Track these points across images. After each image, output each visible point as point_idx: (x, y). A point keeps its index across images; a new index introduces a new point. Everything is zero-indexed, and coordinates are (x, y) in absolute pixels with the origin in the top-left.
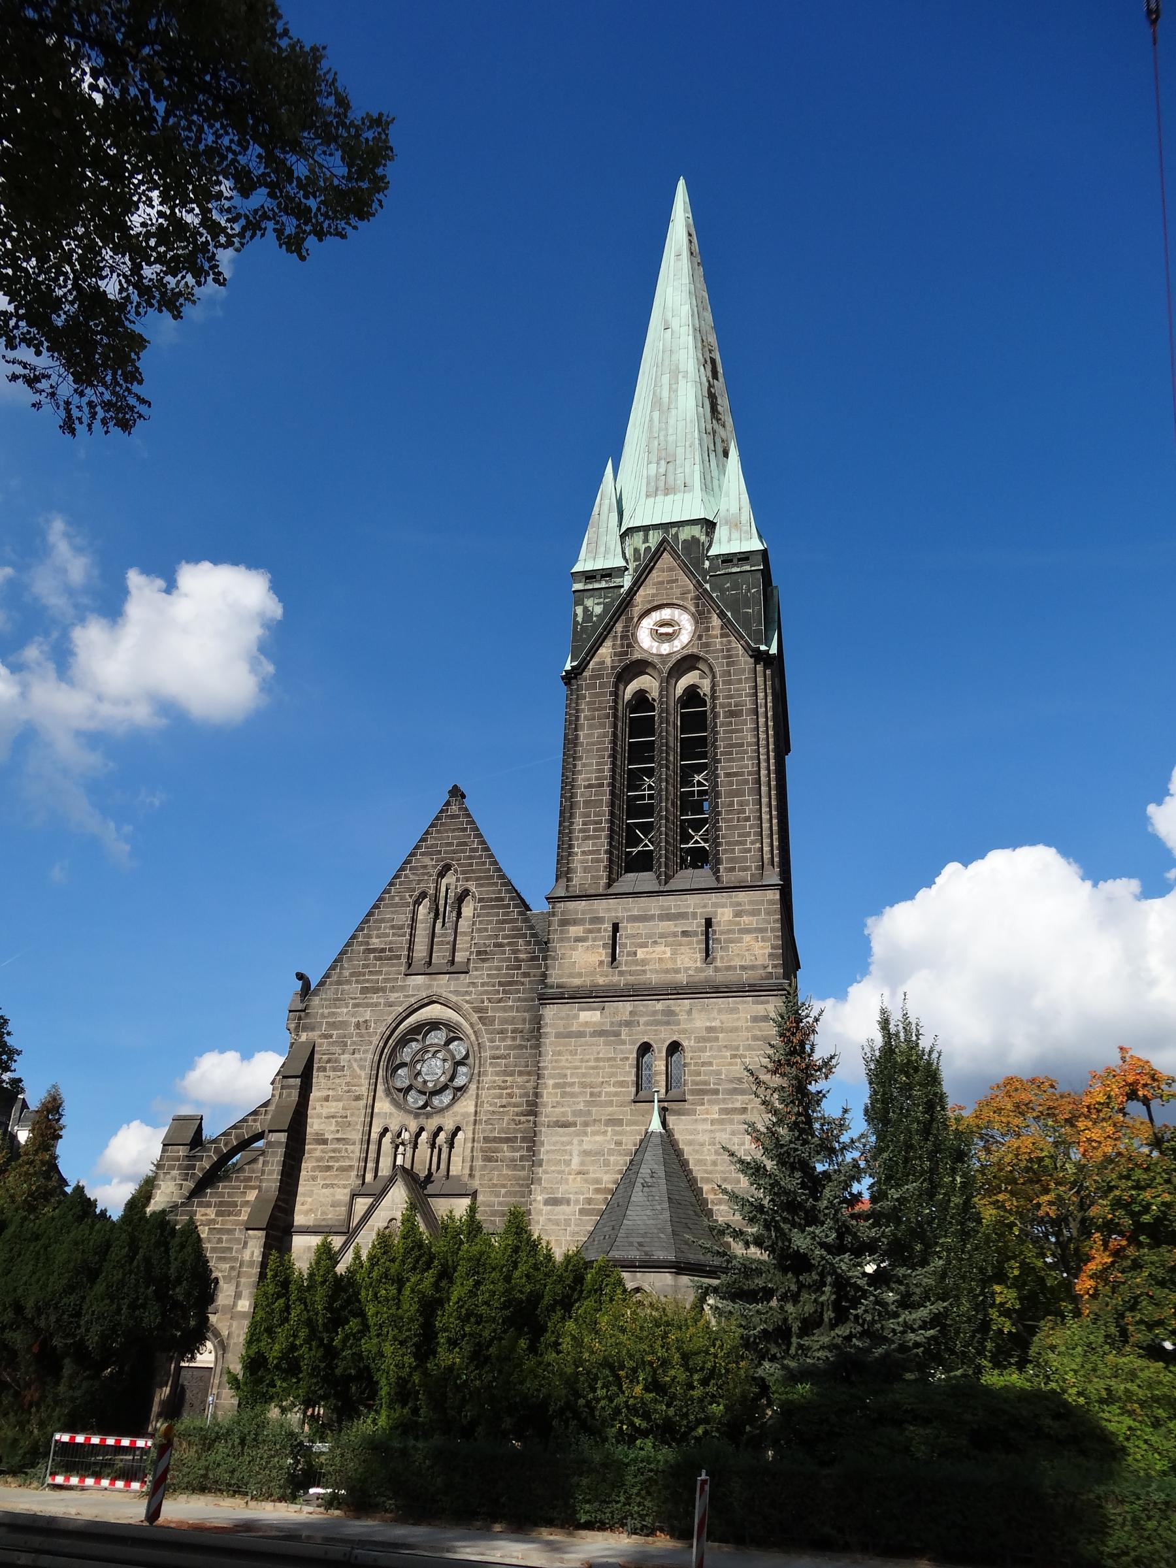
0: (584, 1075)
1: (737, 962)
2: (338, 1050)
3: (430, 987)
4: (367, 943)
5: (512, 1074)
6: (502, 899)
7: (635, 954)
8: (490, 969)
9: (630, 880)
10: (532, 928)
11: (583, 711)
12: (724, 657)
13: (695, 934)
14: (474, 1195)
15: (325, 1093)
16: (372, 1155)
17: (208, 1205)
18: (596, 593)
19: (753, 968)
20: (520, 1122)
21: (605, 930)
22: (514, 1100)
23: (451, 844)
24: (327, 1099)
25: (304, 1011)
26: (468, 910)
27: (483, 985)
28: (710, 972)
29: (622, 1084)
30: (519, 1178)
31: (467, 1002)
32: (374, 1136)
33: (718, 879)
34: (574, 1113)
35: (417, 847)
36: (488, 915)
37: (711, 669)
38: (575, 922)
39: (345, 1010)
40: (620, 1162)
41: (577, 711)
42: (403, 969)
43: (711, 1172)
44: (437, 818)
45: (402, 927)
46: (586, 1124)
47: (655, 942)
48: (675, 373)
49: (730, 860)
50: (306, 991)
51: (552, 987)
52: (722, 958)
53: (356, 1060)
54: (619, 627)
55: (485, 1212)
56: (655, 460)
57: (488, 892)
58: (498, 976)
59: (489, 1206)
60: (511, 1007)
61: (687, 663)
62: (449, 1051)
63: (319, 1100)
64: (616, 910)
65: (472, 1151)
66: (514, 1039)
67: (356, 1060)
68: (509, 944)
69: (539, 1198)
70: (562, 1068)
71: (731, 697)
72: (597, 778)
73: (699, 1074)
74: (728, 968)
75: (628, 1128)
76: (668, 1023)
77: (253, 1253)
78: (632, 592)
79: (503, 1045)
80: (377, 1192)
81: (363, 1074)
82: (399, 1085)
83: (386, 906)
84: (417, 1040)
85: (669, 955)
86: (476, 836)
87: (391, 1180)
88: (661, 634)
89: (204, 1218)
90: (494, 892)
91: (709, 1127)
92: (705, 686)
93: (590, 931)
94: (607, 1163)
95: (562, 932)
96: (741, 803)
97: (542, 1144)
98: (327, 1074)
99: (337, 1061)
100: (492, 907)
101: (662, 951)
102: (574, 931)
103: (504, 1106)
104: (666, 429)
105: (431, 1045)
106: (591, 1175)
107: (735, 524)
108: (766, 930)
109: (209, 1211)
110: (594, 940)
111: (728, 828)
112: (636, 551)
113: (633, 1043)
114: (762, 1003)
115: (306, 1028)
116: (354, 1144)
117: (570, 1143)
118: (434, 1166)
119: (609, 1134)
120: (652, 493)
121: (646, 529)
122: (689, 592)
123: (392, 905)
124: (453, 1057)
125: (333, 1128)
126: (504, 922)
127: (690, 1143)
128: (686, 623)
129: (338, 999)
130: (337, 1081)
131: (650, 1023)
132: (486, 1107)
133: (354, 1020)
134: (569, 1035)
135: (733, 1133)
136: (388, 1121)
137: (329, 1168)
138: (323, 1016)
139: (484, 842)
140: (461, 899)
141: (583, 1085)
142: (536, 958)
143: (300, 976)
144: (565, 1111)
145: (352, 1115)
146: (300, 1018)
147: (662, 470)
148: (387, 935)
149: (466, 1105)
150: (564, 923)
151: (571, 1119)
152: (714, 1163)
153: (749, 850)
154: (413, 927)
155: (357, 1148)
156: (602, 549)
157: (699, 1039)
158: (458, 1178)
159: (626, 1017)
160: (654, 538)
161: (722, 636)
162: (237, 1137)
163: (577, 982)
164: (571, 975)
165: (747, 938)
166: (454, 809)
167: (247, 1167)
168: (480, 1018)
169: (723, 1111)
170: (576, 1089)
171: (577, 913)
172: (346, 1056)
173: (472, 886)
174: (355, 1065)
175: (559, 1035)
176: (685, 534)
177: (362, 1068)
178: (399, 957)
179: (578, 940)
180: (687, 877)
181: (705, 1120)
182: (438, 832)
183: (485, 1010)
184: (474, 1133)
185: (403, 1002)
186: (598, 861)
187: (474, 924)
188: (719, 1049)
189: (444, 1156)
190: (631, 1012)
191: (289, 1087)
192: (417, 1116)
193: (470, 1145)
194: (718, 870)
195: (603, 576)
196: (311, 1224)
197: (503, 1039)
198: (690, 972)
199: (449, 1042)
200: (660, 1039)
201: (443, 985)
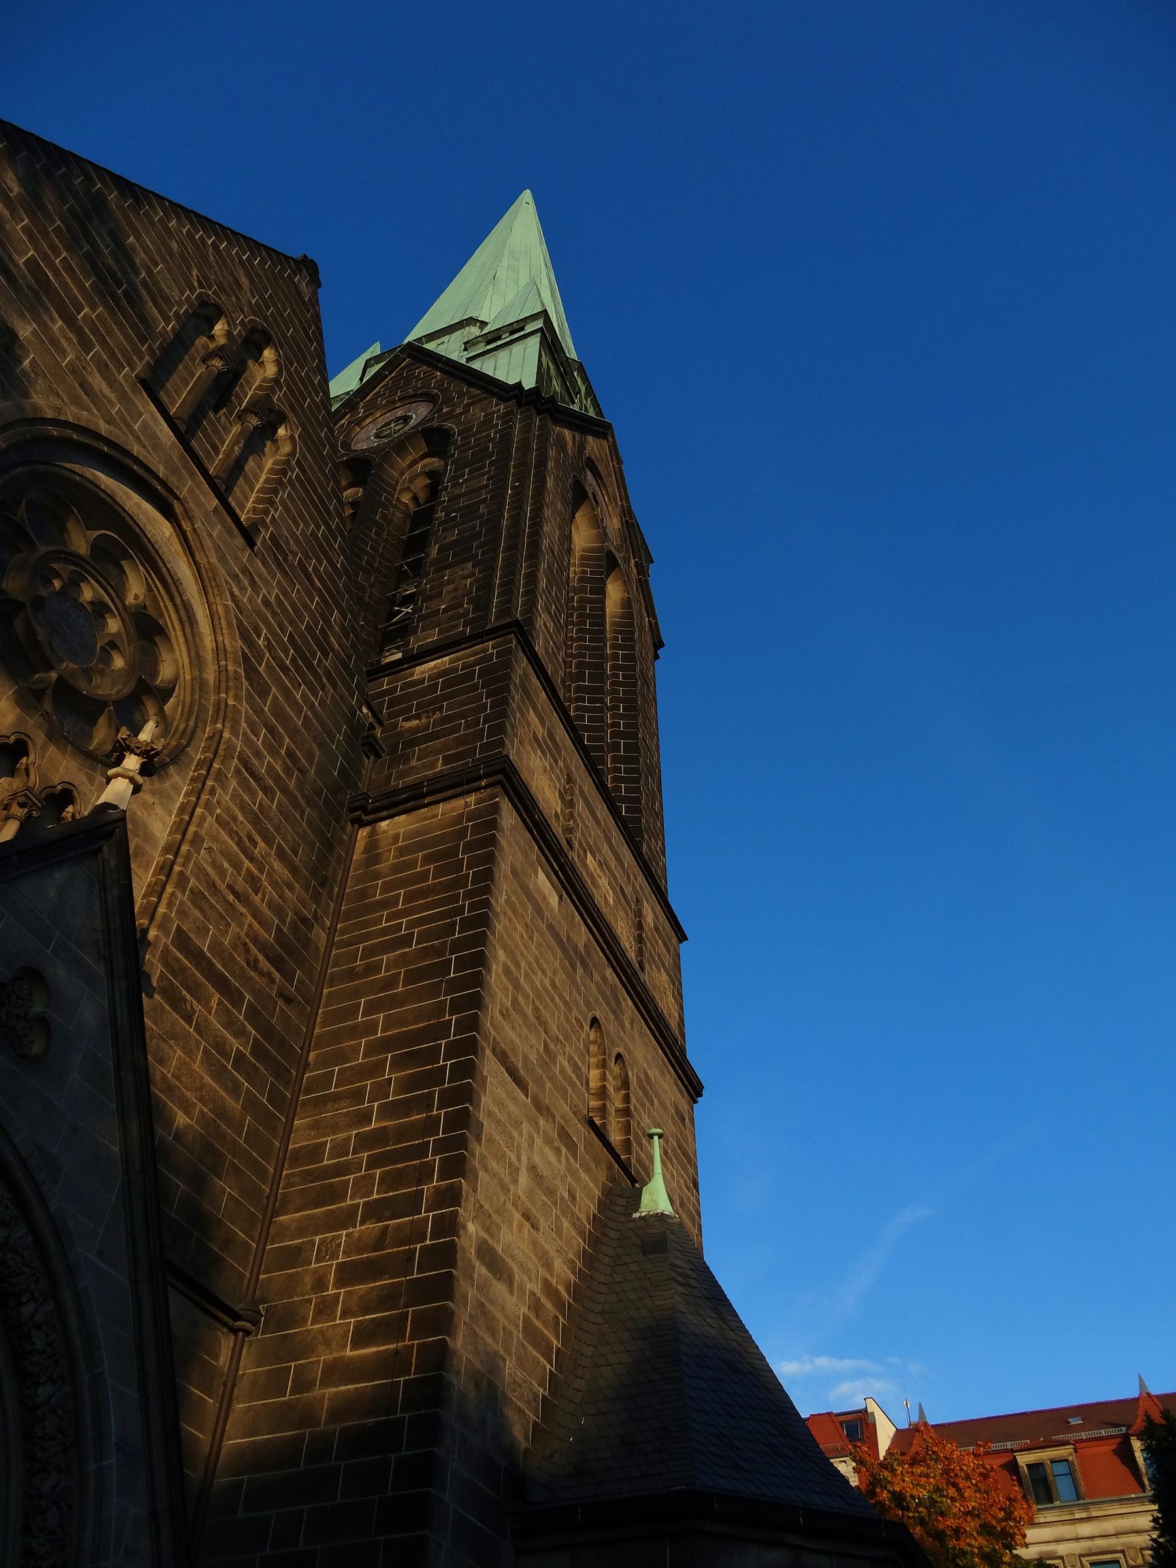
5: (269, 841)
20: (254, 965)
27: (266, 602)
45: (167, 300)
66: (287, 770)
69: (471, 1227)
197: (274, 752)
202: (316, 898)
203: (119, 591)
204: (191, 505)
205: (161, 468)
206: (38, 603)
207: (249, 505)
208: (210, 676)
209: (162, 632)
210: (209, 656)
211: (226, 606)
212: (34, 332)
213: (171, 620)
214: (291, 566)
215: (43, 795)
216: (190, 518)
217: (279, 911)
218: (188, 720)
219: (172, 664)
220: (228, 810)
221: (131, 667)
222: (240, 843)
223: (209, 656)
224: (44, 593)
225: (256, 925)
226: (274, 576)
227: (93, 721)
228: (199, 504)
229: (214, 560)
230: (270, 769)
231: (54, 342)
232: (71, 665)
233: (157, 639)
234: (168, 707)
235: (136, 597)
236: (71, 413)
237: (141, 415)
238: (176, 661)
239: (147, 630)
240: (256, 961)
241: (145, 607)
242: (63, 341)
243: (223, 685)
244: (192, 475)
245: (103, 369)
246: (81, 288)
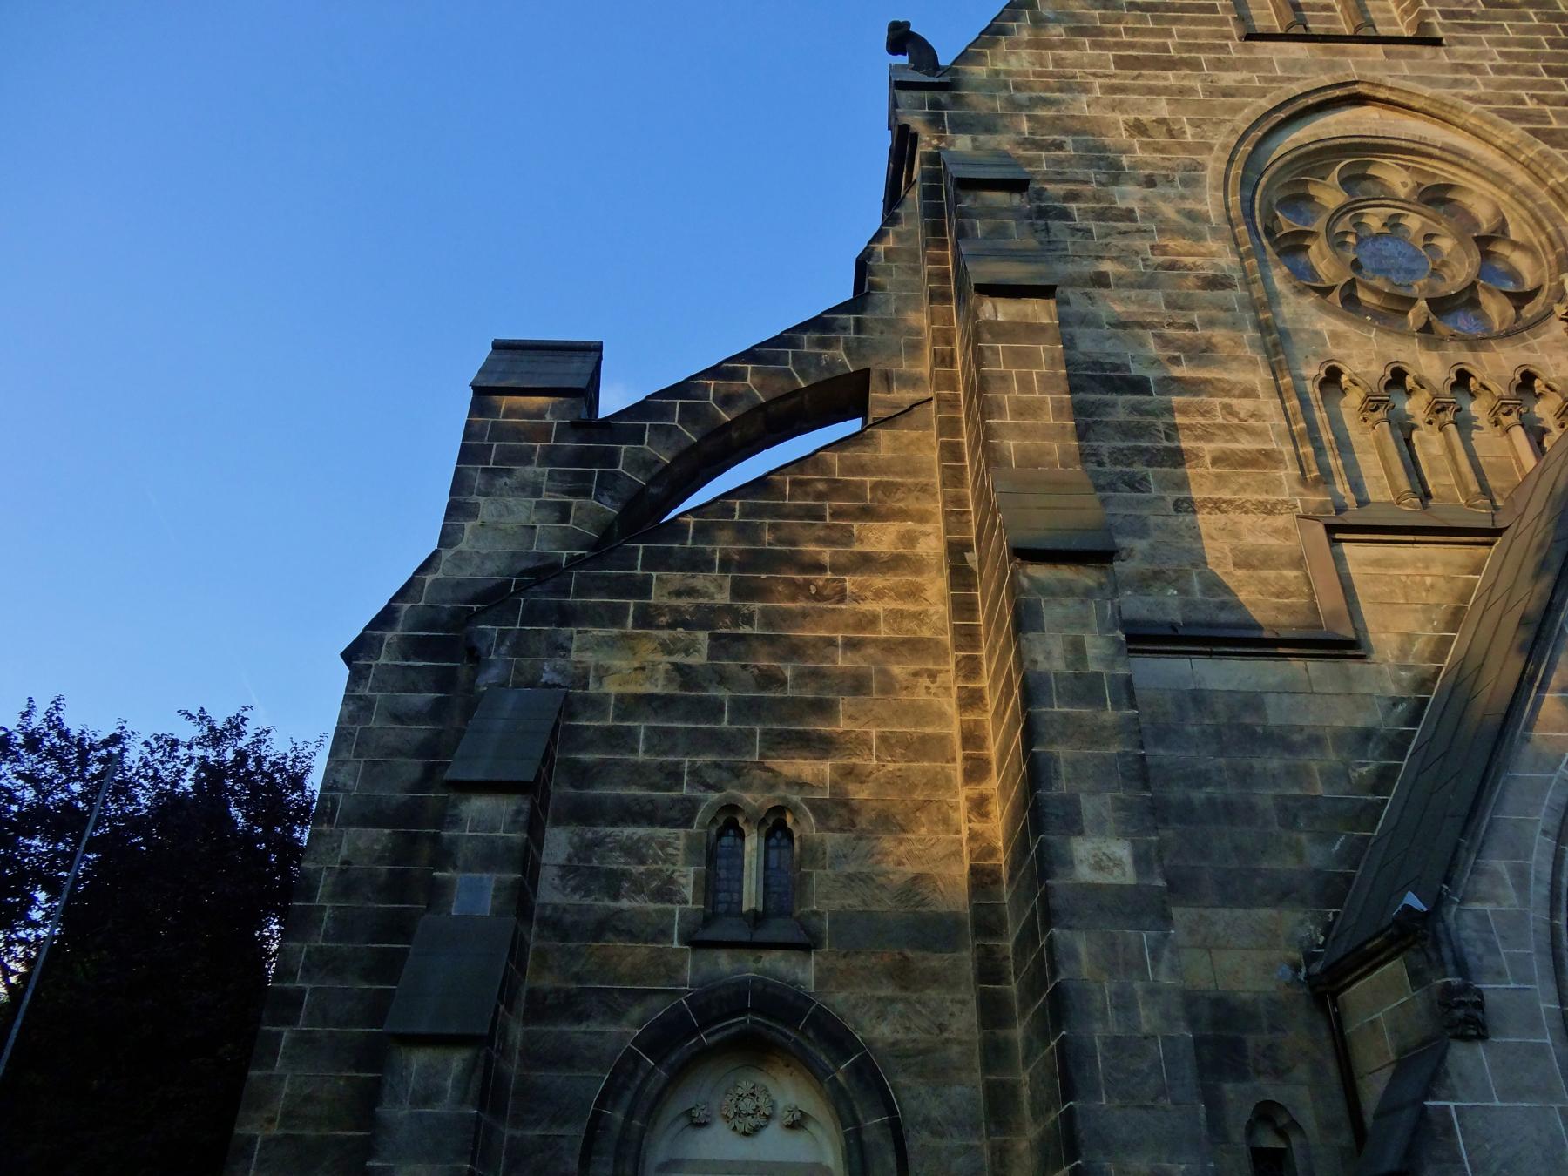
17: (697, 563)
27: (1499, 70)
77: (1077, 648)
89: (683, 602)
109: (699, 580)
116: (1249, 393)
143: (901, 38)
196: (1177, 617)
203: (1388, 197)
204: (1369, 75)
205: (1323, 77)
206: (1356, 265)
207: (1396, 13)
208: (1521, 178)
209: (1449, 187)
210: (1503, 165)
211: (1475, 114)
212: (1169, 102)
213: (1445, 172)
214: (1484, 15)
215: (1513, 391)
216: (1379, 85)
218: (1543, 229)
219: (1481, 202)
221: (1460, 238)
223: (1503, 165)
224: (1352, 256)
226: (1479, 42)
227: (1474, 303)
228: (1373, 67)
229: (1428, 91)
231: (1182, 91)
232: (1421, 283)
233: (1449, 196)
234: (1513, 236)
235: (1404, 184)
236: (1241, 121)
237: (1270, 61)
238: (1482, 196)
239: (1436, 197)
241: (1420, 185)
242: (1186, 83)
243: (1542, 174)
244: (1343, 53)
245: (1219, 65)
246: (1151, 32)
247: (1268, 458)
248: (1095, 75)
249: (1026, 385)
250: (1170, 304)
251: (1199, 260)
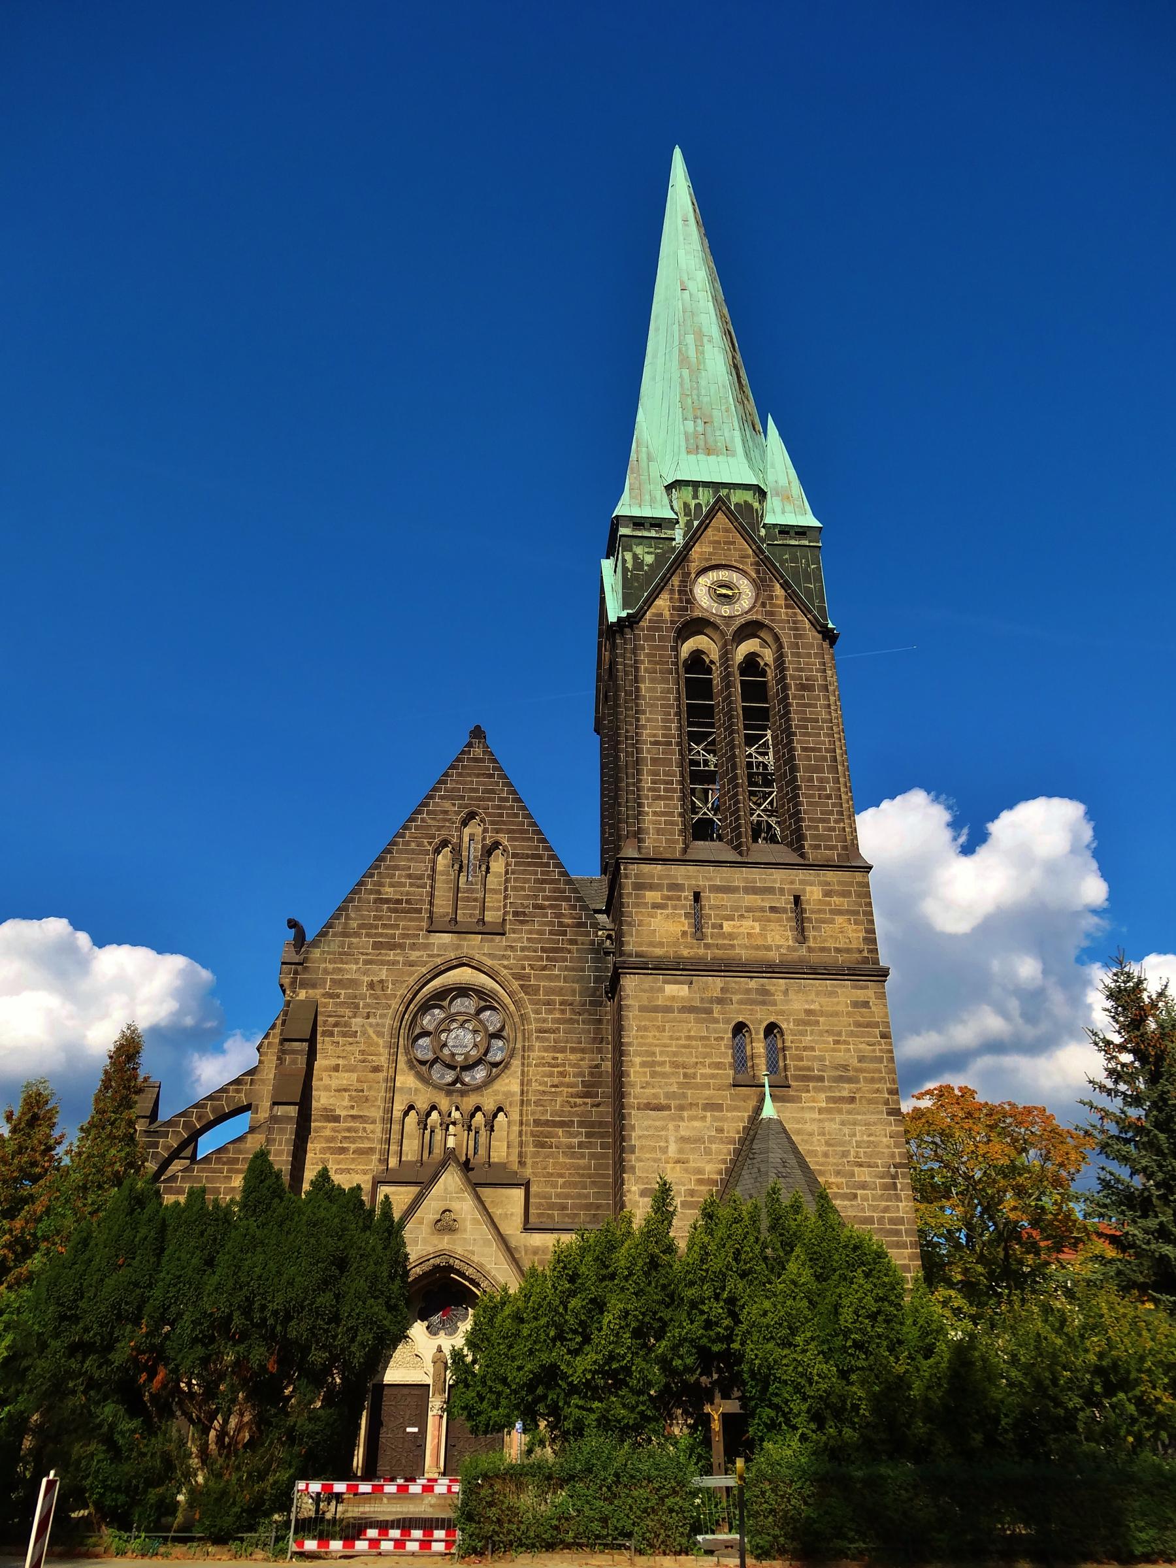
0: (675, 1054)
1: (830, 944)
2: (347, 1012)
3: (458, 947)
4: (379, 892)
5: (563, 1050)
6: (540, 857)
7: (721, 927)
8: (530, 932)
9: (702, 848)
10: (576, 891)
11: (643, 662)
12: (790, 629)
13: (785, 910)
14: (527, 1185)
15: (334, 1061)
16: (395, 1137)
18: (645, 541)
19: (848, 951)
20: (576, 1105)
21: (686, 898)
22: (567, 1079)
23: (476, 790)
24: (336, 1068)
25: (301, 964)
26: (498, 865)
27: (523, 949)
28: (803, 952)
29: (718, 1065)
30: (579, 1167)
31: (505, 967)
32: (397, 1114)
33: (802, 856)
34: (668, 1096)
35: (434, 789)
36: (524, 872)
37: (777, 638)
38: (651, 887)
39: (354, 967)
40: (723, 1151)
41: (636, 661)
42: (424, 924)
43: (822, 1165)
44: (458, 760)
45: (421, 877)
46: (681, 1108)
47: (742, 916)
48: (699, 335)
49: (814, 837)
50: (300, 939)
51: (630, 955)
52: (814, 938)
53: (371, 1025)
54: (676, 581)
55: (541, 1204)
56: (691, 416)
57: (523, 847)
58: (539, 941)
59: (545, 1198)
60: (558, 976)
61: (750, 629)
62: (481, 1021)
63: (327, 1069)
64: (696, 878)
65: (520, 1133)
66: (563, 1012)
67: (371, 1025)
68: (551, 907)
69: (634, 1188)
70: (651, 1045)
71: (801, 670)
72: (664, 736)
73: (801, 1059)
74: (823, 949)
75: (729, 1114)
76: (764, 1003)
78: (688, 547)
79: (551, 1018)
80: (425, 1179)
81: (381, 1042)
82: (420, 1056)
83: (400, 852)
84: (441, 1007)
85: (757, 930)
86: (504, 785)
87: (443, 1165)
88: (720, 595)
90: (529, 848)
91: (817, 1116)
92: (768, 656)
93: (669, 898)
94: (708, 1152)
95: (637, 897)
96: (821, 780)
97: (633, 1127)
98: (336, 1039)
99: (347, 1025)
100: (529, 864)
101: (749, 926)
102: (651, 896)
103: (556, 1086)
104: (698, 389)
105: (459, 1013)
106: (692, 1164)
107: (787, 498)
108: (858, 913)
110: (675, 907)
111: (810, 804)
112: (686, 505)
113: (727, 1021)
114: (862, 988)
115: (304, 985)
116: (374, 1122)
117: (664, 1128)
118: (471, 1152)
119: (709, 1119)
120: (693, 450)
121: (696, 484)
122: (748, 556)
123: (407, 852)
124: (486, 1030)
125: (346, 1103)
126: (543, 881)
127: (799, 1132)
128: (745, 587)
129: (345, 953)
130: (348, 1048)
131: (742, 1000)
132: (535, 1086)
133: (366, 979)
134: (656, 1009)
135: (843, 1123)
136: (414, 1098)
137: (343, 1150)
138: (326, 971)
139: (514, 792)
140: (489, 851)
141: (675, 1065)
142: (584, 925)
143: (292, 924)
144: (656, 1092)
145: (370, 1089)
146: (296, 973)
147: (700, 429)
148: (403, 885)
149: (509, 1084)
150: (638, 887)
151: (663, 1102)
152: (826, 1155)
153: (834, 829)
154: (432, 878)
155: (378, 1127)
156: (647, 497)
157: (798, 1022)
158: (503, 1166)
159: (717, 993)
160: (706, 497)
161: (787, 607)
162: (214, 1110)
163: (659, 951)
164: (651, 944)
165: (839, 919)
166: (477, 751)
167: (231, 1147)
168: (522, 986)
169: (829, 1099)
170: (667, 1069)
171: (652, 877)
172: (358, 1020)
173: (504, 839)
174: (370, 1031)
175: (642, 1009)
176: (737, 497)
177: (380, 1034)
178: (419, 911)
179: (656, 906)
180: (762, 850)
181: (813, 1108)
182: (459, 775)
183: (528, 977)
184: (521, 1115)
185: (426, 963)
186: (673, 823)
187: (507, 881)
188: (821, 1033)
189: (482, 1139)
190: (722, 989)
191: (294, 1052)
192: (449, 1093)
193: (516, 1128)
194: (802, 847)
195: (653, 525)
197: (550, 1012)
198: (783, 951)
199: (480, 1011)
200: (758, 1018)
201: (474, 945)
202: (600, 1051)
217: (581, 1074)
220: (539, 1058)
222: (550, 1065)
225: (570, 1090)
230: (555, 1021)
240: (575, 1103)
245: (413, 947)
247: (371, 1150)
248: (362, 954)
249: (280, 1145)
250: (359, 1081)
251: (374, 1058)
